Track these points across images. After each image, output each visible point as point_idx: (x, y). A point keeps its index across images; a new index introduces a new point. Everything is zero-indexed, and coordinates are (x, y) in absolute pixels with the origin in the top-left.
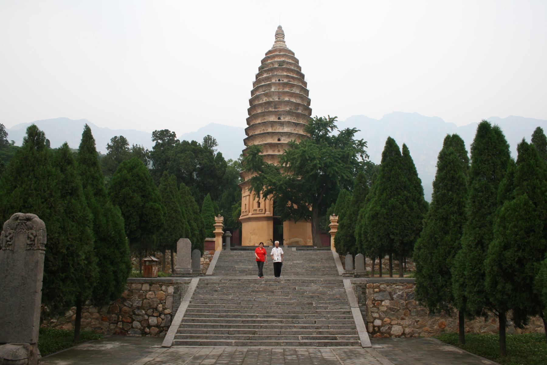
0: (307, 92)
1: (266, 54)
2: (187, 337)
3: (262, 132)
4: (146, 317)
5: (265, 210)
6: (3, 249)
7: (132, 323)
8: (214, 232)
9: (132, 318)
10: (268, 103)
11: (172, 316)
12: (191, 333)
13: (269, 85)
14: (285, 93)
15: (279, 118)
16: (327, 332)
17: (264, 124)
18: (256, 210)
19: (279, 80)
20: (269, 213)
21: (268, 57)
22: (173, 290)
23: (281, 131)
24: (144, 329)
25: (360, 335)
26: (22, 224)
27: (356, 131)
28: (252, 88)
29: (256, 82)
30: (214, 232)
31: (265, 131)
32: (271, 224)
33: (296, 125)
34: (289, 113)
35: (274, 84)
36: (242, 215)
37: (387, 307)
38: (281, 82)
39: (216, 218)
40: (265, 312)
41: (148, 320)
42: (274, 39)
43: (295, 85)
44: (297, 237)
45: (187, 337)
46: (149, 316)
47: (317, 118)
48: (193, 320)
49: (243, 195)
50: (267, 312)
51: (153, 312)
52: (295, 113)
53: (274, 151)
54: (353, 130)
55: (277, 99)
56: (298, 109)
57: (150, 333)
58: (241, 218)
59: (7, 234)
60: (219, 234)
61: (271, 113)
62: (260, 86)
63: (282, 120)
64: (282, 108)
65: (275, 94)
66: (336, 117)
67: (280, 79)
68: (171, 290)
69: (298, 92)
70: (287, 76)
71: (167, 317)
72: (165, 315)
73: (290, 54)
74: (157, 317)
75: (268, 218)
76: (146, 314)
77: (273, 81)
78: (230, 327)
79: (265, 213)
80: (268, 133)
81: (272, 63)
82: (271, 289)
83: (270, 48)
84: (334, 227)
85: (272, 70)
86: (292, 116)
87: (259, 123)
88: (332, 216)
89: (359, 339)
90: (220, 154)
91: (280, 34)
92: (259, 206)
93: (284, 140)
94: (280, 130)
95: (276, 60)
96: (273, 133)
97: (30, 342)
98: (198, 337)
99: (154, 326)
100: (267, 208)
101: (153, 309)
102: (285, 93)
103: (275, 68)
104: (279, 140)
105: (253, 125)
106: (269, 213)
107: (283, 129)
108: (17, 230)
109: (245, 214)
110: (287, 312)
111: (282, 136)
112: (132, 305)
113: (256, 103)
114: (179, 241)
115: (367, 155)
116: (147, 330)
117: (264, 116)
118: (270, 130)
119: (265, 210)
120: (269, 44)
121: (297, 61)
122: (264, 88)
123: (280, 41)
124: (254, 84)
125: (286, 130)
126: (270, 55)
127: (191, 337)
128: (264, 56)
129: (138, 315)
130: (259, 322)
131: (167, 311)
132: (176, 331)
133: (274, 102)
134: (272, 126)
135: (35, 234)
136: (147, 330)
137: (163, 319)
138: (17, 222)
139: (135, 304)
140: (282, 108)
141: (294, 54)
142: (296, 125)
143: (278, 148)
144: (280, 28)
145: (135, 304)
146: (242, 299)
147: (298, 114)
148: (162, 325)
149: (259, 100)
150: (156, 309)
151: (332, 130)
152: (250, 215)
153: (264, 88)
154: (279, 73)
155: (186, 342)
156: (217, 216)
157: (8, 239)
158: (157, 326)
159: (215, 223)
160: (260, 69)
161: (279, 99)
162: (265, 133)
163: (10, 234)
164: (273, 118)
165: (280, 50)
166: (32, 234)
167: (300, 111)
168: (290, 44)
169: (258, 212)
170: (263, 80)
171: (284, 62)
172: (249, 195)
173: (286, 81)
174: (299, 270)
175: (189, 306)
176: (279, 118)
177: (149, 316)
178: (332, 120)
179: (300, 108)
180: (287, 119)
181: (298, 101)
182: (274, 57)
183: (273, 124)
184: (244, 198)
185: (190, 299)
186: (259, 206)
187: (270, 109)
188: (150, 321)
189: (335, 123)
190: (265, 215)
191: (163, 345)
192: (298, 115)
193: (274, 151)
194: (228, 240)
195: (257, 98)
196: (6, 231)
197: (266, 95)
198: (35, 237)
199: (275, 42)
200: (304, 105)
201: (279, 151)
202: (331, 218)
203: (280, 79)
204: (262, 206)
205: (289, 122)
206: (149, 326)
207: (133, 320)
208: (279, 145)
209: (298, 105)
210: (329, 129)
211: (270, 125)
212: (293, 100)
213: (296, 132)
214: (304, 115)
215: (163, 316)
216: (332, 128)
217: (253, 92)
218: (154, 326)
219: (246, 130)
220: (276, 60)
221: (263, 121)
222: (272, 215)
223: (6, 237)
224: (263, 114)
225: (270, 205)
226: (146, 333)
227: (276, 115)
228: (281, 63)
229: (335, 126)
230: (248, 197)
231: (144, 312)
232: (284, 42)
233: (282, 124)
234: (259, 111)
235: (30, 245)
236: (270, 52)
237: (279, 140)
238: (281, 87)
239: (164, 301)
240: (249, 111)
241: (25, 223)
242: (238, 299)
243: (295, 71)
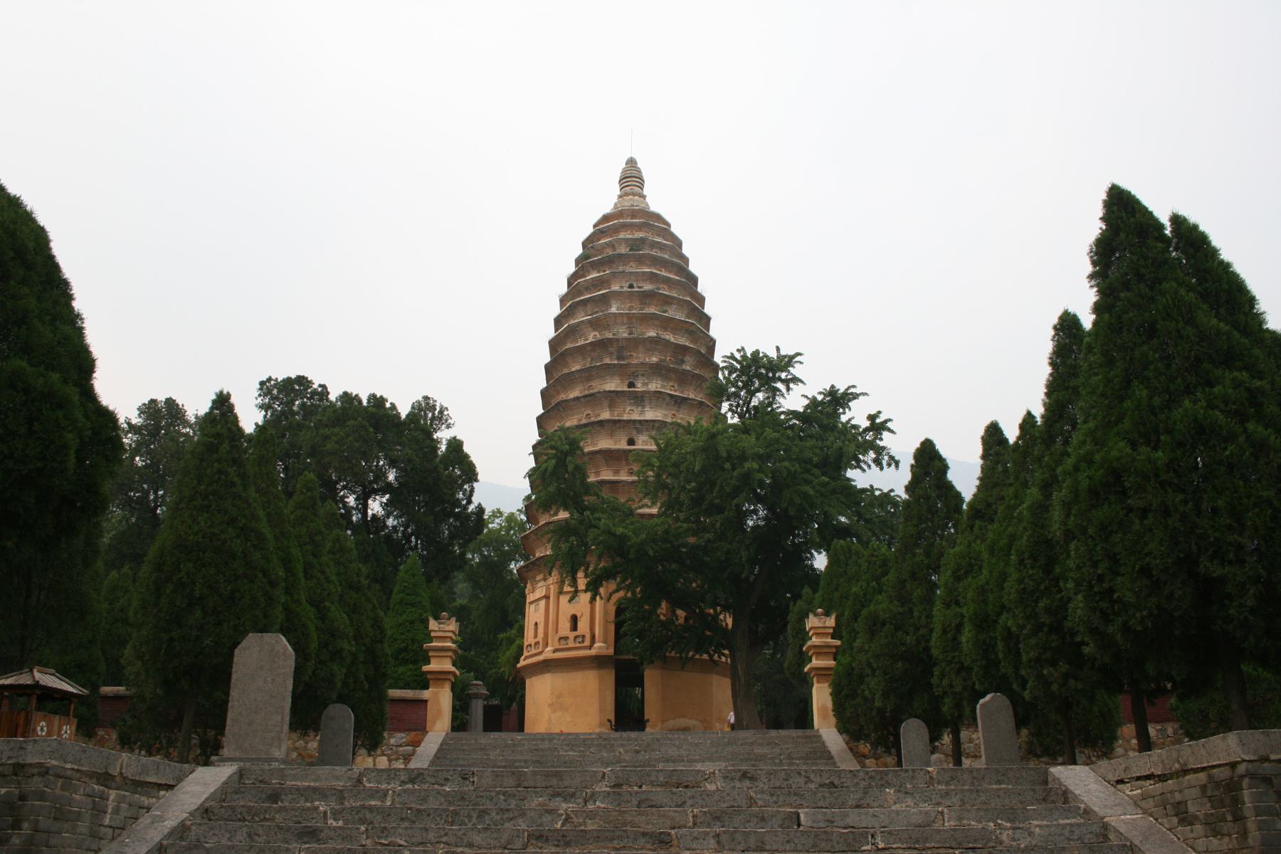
0: (706, 320)
1: (595, 226)
3: (584, 421)
5: (593, 637)
8: (425, 668)
10: (601, 345)
13: (605, 300)
14: (647, 319)
15: (631, 385)
17: (591, 399)
18: (566, 638)
19: (631, 286)
23: (636, 417)
27: (856, 396)
28: (557, 310)
29: (566, 295)
30: (425, 668)
31: (593, 419)
32: (610, 676)
33: (679, 402)
34: (657, 370)
36: (526, 654)
39: (433, 625)
42: (617, 191)
43: (673, 298)
44: (683, 716)
47: (744, 357)
49: (530, 598)
52: (675, 371)
53: (616, 472)
54: (845, 394)
55: (625, 335)
56: (683, 362)
58: (522, 663)
60: (440, 676)
61: (607, 370)
62: (578, 303)
63: (640, 387)
64: (642, 357)
65: (619, 320)
66: (798, 354)
67: (631, 283)
69: (680, 316)
70: (653, 277)
73: (656, 224)
77: (615, 288)
79: (590, 647)
80: (601, 423)
81: (611, 245)
82: (653, 823)
83: (608, 208)
84: (821, 651)
85: (609, 261)
86: (666, 378)
87: (577, 398)
88: (816, 615)
90: (456, 445)
91: (631, 178)
92: (574, 628)
93: (645, 443)
94: (632, 413)
95: (622, 236)
96: (615, 422)
102: (647, 319)
103: (620, 256)
104: (631, 442)
105: (558, 404)
106: (601, 647)
107: (642, 413)
109: (533, 651)
111: (639, 431)
114: (244, 643)
115: (892, 458)
117: (589, 379)
118: (606, 415)
119: (593, 637)
120: (606, 199)
121: (679, 244)
122: (589, 307)
123: (634, 194)
124: (563, 300)
125: (650, 414)
126: (606, 227)
128: (591, 230)
133: (617, 340)
134: (612, 407)
140: (642, 357)
141: (669, 225)
142: (679, 402)
143: (628, 464)
144: (631, 162)
147: (684, 372)
151: (788, 389)
152: (548, 653)
154: (632, 268)
156: (436, 618)
159: (431, 640)
160: (578, 261)
161: (631, 333)
162: (592, 424)
164: (612, 385)
165: (634, 213)
168: (656, 199)
169: (571, 644)
171: (643, 240)
172: (547, 597)
173: (648, 287)
176: (631, 385)
178: (786, 362)
179: (687, 358)
181: (683, 341)
182: (616, 229)
183: (613, 398)
184: (532, 607)
186: (574, 628)
187: (607, 361)
189: (796, 371)
190: (593, 652)
192: (683, 378)
193: (616, 472)
194: (478, 708)
195: (572, 332)
197: (594, 324)
199: (620, 197)
200: (699, 352)
203: (631, 283)
204: (583, 626)
205: (658, 395)
209: (684, 349)
210: (779, 385)
211: (606, 403)
212: (670, 337)
214: (699, 377)
216: (786, 382)
217: (558, 322)
220: (622, 236)
222: (611, 651)
224: (587, 375)
225: (606, 622)
228: (636, 245)
229: (796, 380)
230: (543, 603)
232: (644, 197)
233: (639, 399)
236: (606, 218)
237: (631, 442)
238: (636, 304)
240: (549, 369)
243: (673, 264)
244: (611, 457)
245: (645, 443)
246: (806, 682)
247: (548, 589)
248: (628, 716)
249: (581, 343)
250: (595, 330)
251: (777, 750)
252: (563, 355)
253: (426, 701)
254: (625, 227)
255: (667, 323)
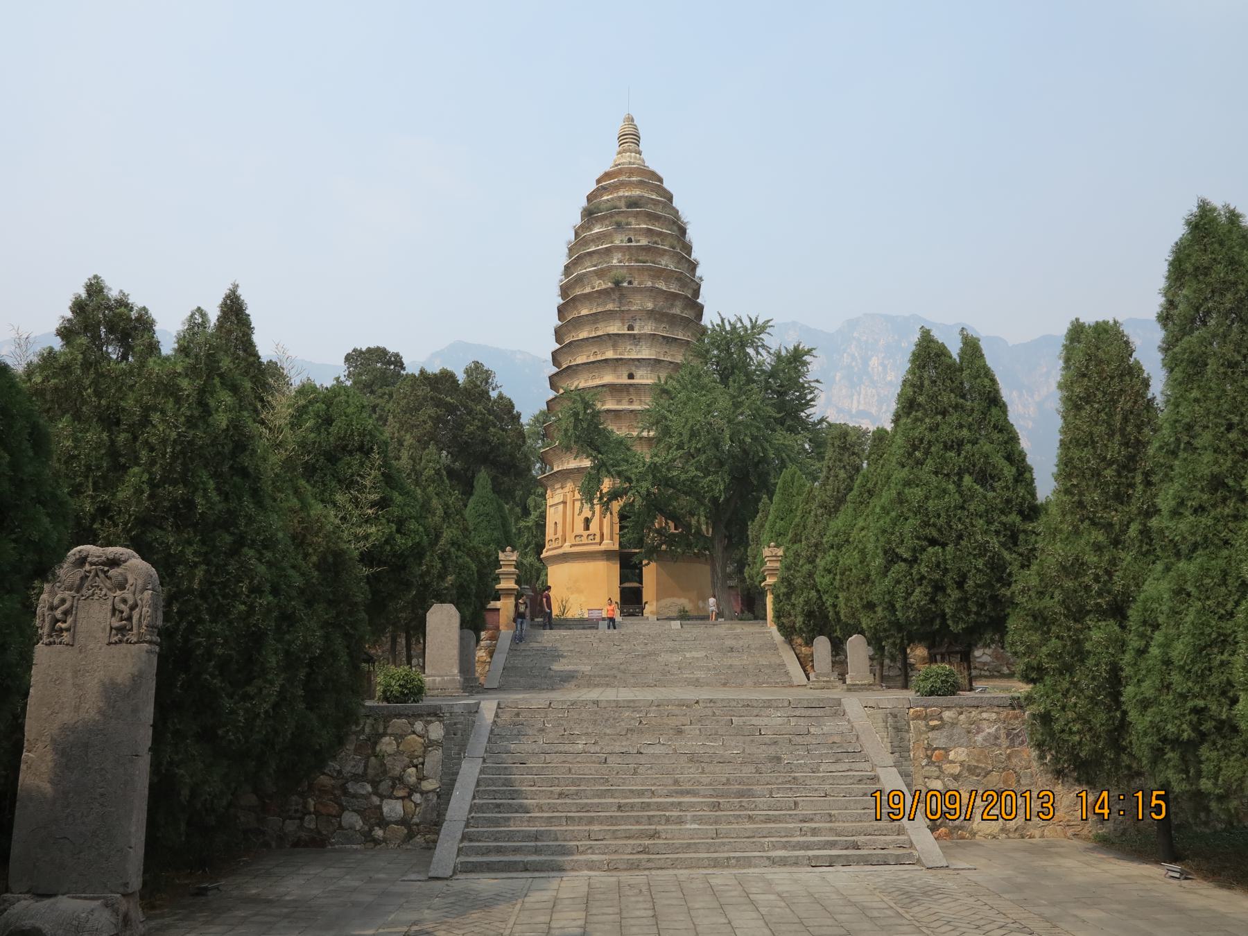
0: (693, 266)
1: (598, 181)
2: (488, 851)
3: (592, 359)
4: (376, 800)
5: (602, 535)
6: (45, 640)
7: (340, 816)
8: (498, 587)
9: (340, 805)
11: (444, 795)
12: (496, 840)
15: (631, 328)
16: (831, 829)
19: (630, 240)
20: (611, 544)
21: (604, 188)
22: (442, 733)
24: (371, 830)
25: (913, 838)
26: (97, 575)
28: (565, 261)
31: (599, 358)
32: (615, 568)
33: (668, 341)
34: (651, 314)
35: (618, 248)
36: (547, 547)
37: (962, 764)
38: (633, 244)
39: (501, 556)
40: (671, 781)
41: (380, 807)
43: (665, 251)
45: (488, 851)
46: (382, 797)
48: (498, 806)
49: (550, 502)
50: (676, 782)
51: (393, 787)
52: (666, 315)
53: (619, 402)
57: (385, 840)
59: (56, 602)
60: (508, 592)
61: (609, 315)
68: (436, 731)
69: (672, 267)
71: (427, 800)
72: (422, 793)
73: (652, 180)
74: (403, 798)
75: (608, 555)
76: (376, 793)
77: (617, 242)
78: (591, 821)
80: (606, 360)
82: (673, 722)
83: (607, 167)
84: (773, 572)
89: (912, 845)
91: (631, 138)
92: (587, 528)
95: (621, 194)
97: (121, 890)
98: (516, 850)
99: (396, 823)
100: (606, 531)
101: (393, 779)
104: (631, 376)
106: (611, 544)
108: (84, 591)
109: (554, 545)
110: (724, 780)
112: (339, 772)
113: (578, 292)
116: (379, 833)
117: (595, 322)
118: (610, 354)
119: (602, 535)
121: (670, 198)
125: (646, 353)
126: (607, 181)
127: (499, 850)
128: (594, 186)
129: (354, 796)
130: (660, 807)
131: (428, 785)
132: (459, 836)
134: (615, 347)
135: (130, 602)
136: (379, 833)
137: (416, 805)
138: (80, 572)
139: (348, 769)
141: (661, 180)
142: (668, 341)
145: (349, 768)
146: (608, 749)
147: (674, 316)
148: (416, 820)
149: (584, 286)
150: (399, 780)
152: (566, 548)
153: (595, 259)
155: (488, 863)
156: (504, 551)
157: (58, 613)
158: (403, 822)
163: (63, 601)
164: (614, 328)
165: (631, 172)
166: (124, 601)
167: (677, 311)
169: (584, 540)
170: (593, 240)
172: (564, 503)
173: (644, 242)
174: (700, 674)
175: (482, 771)
176: (631, 328)
177: (382, 797)
180: (648, 328)
181: (674, 288)
182: (616, 187)
183: (614, 339)
184: (552, 509)
185: (482, 753)
186: (587, 528)
188: (385, 809)
190: (603, 547)
191: (430, 874)
192: (673, 320)
195: (580, 280)
196: (53, 593)
197: (600, 274)
198: (132, 608)
200: (687, 297)
201: (631, 402)
202: (766, 552)
204: (594, 526)
206: (383, 823)
207: (343, 809)
208: (631, 389)
209: (675, 296)
212: (662, 285)
213: (669, 359)
215: (417, 797)
217: (568, 269)
218: (396, 823)
219: (555, 355)
221: (593, 335)
222: (616, 547)
223: (52, 608)
224: (595, 318)
226: (376, 842)
227: (623, 320)
228: (633, 203)
230: (561, 507)
231: (369, 788)
232: (640, 153)
233: (636, 339)
234: (584, 312)
235: (121, 630)
236: (607, 175)
237: (631, 376)
239: (421, 760)
240: (561, 311)
241: (105, 572)
242: (597, 749)
244: (617, 414)
245: (644, 378)
246: (763, 594)
247: (565, 496)
248: (631, 600)
249: (588, 290)
250: (600, 278)
251: (741, 642)
252: (574, 299)
253: (498, 610)
254: (622, 185)
255: (659, 273)
